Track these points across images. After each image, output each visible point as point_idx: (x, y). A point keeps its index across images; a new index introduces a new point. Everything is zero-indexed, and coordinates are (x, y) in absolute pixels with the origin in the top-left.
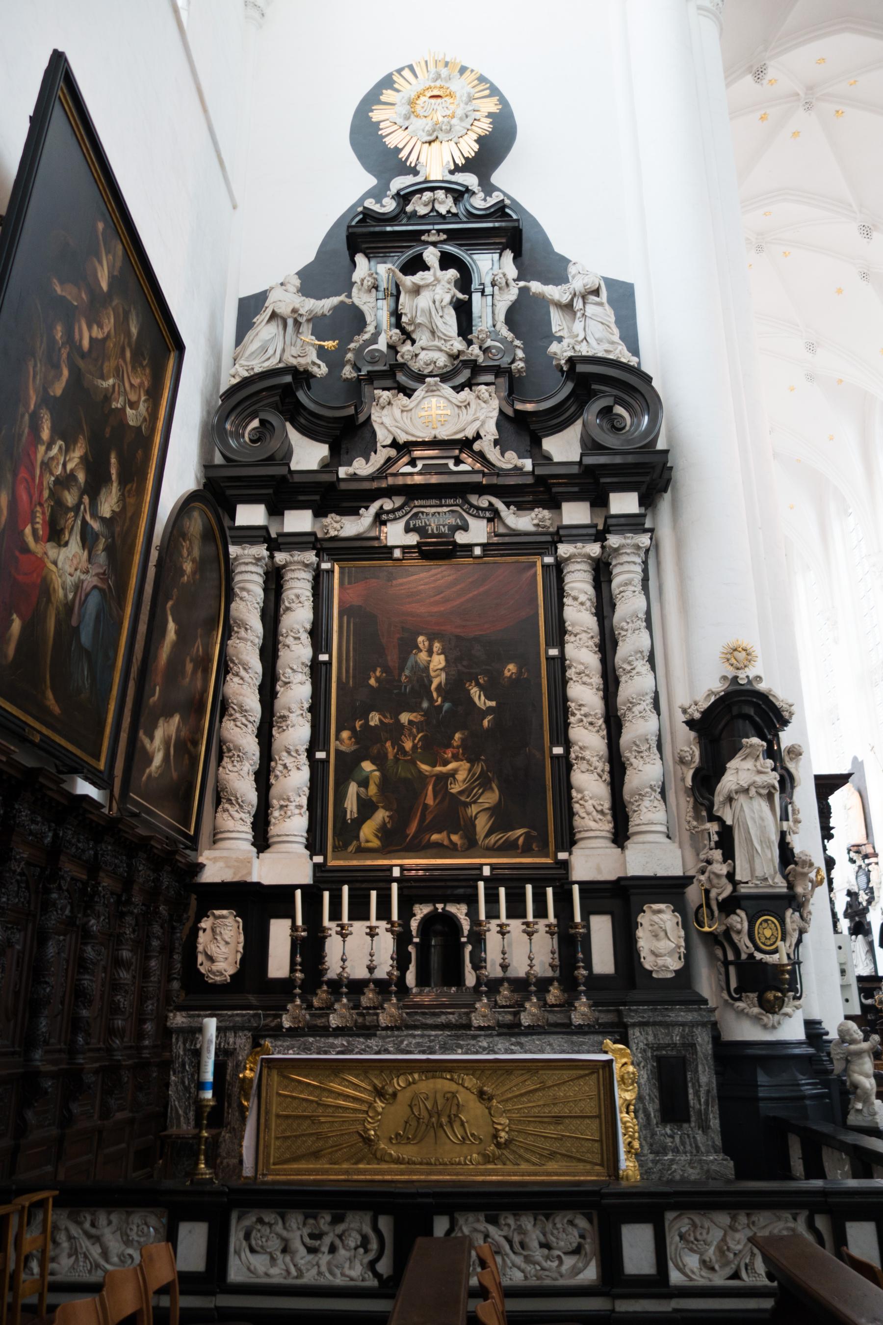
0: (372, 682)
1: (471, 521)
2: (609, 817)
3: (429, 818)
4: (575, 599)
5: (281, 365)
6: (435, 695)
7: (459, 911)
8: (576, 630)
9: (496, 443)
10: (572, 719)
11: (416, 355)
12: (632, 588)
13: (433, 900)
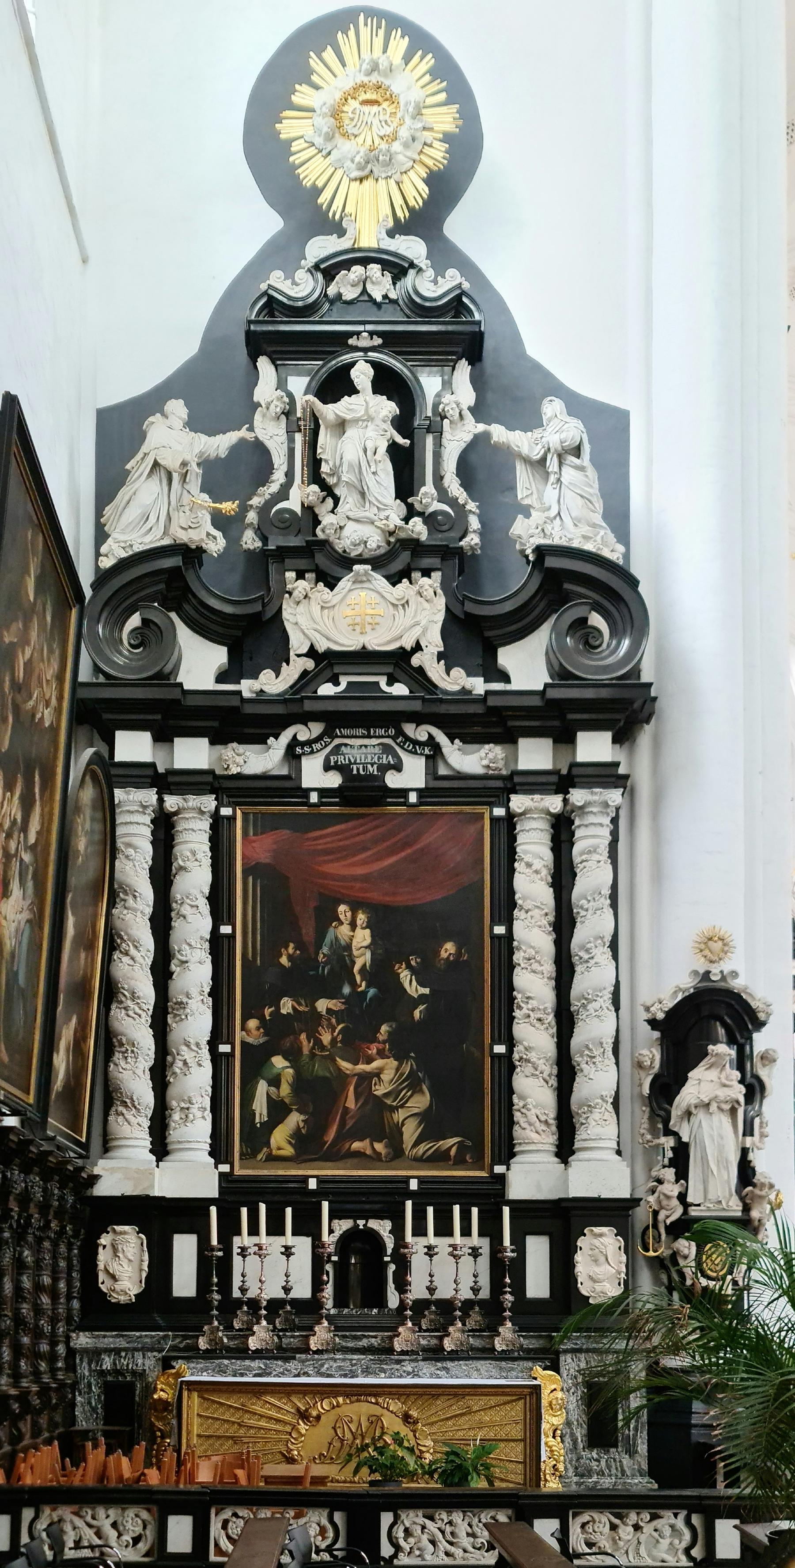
0: (284, 960)
1: (405, 757)
2: (554, 1128)
3: (350, 1123)
4: (529, 865)
5: (166, 542)
6: (358, 978)
7: (383, 1227)
8: (528, 905)
9: (440, 656)
10: (517, 1013)
11: (341, 528)
12: (596, 857)
13: (355, 1219)
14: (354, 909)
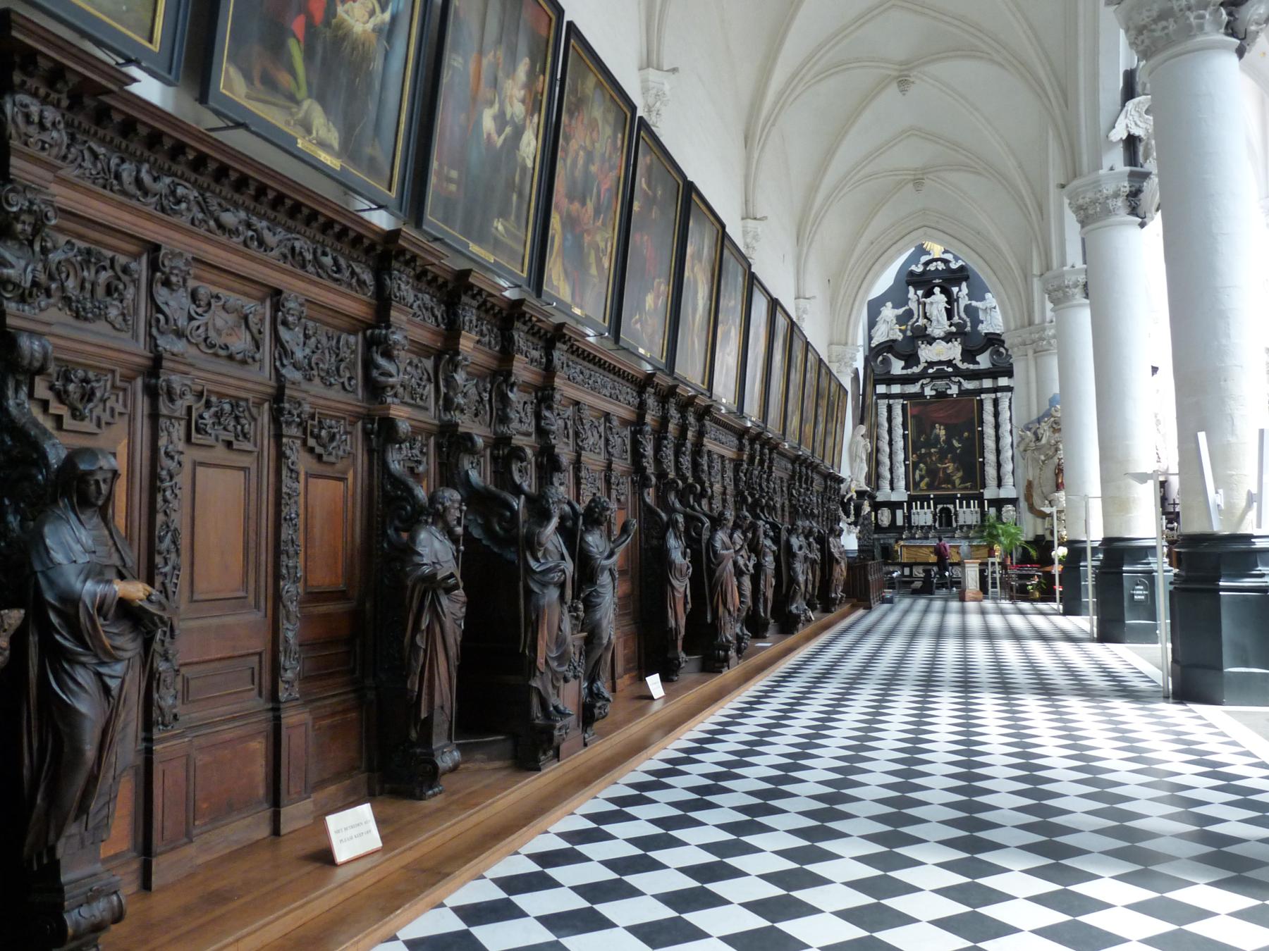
7: (951, 507)
14: (940, 425)
